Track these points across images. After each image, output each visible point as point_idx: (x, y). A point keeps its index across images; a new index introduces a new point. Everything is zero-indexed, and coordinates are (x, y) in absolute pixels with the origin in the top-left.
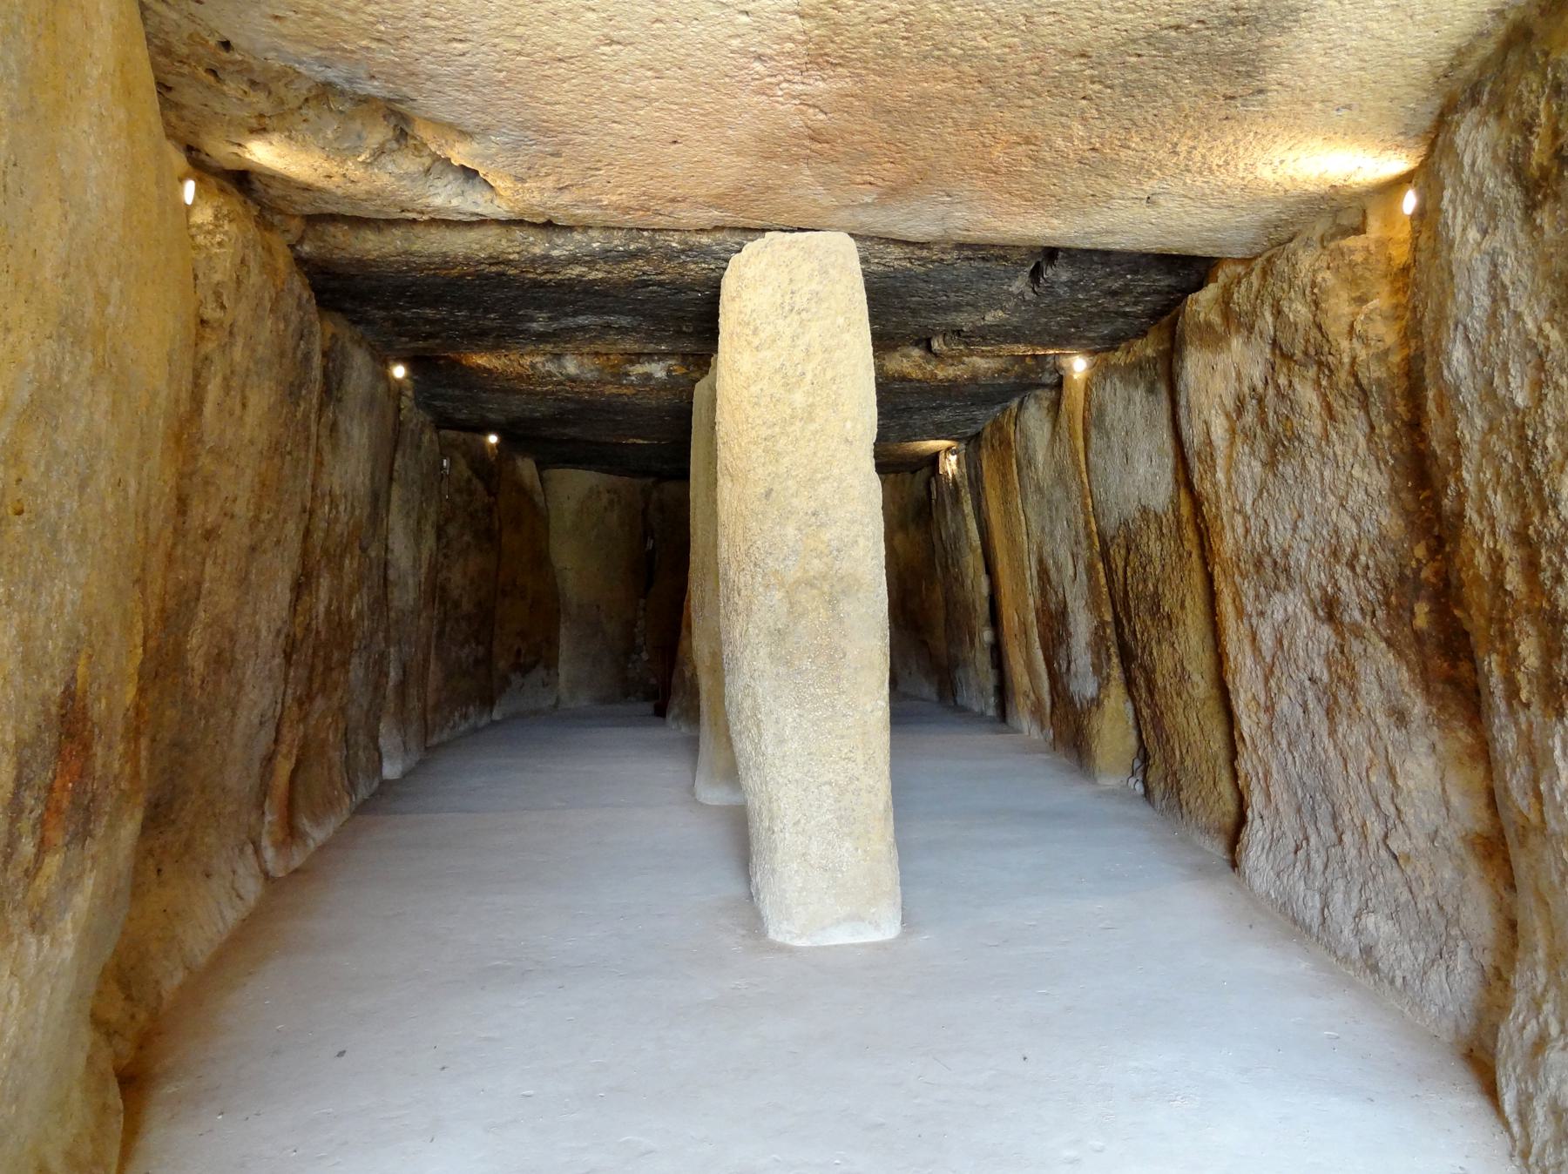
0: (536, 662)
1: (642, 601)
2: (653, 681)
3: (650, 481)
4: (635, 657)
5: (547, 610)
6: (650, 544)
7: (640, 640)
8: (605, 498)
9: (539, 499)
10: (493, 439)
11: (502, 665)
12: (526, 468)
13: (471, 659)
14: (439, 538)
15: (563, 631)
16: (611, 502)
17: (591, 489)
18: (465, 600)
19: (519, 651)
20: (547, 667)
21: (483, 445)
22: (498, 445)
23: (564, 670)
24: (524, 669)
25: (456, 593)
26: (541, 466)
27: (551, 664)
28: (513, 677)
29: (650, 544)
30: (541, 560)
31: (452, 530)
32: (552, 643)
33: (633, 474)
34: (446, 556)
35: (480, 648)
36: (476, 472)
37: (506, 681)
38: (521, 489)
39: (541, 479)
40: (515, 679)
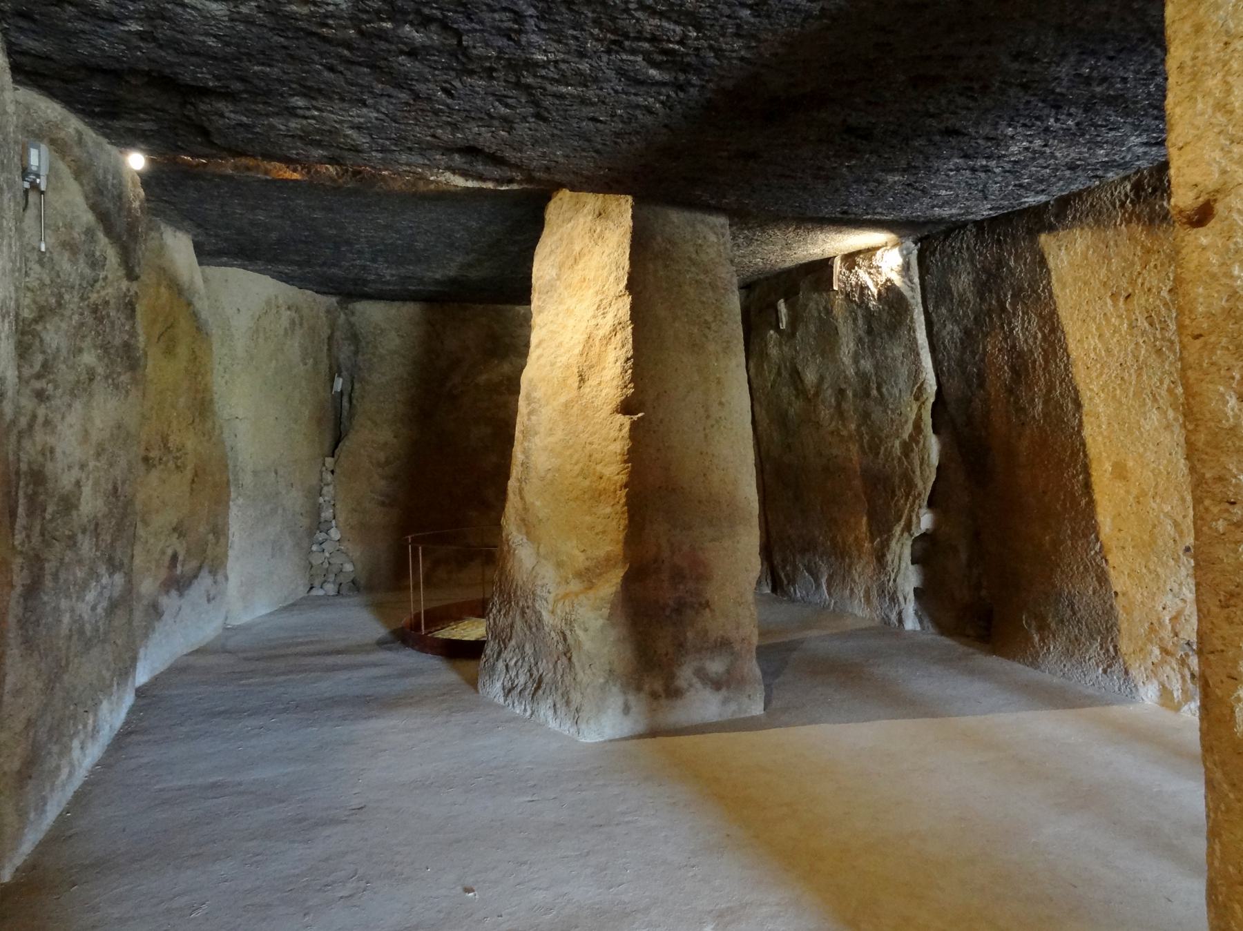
0: (200, 568)
1: (329, 460)
2: (348, 567)
3: (333, 300)
4: (321, 536)
5: (211, 482)
6: (339, 384)
7: (327, 514)
8: (286, 315)
9: (202, 305)
10: (136, 161)
11: (147, 586)
12: (178, 247)
13: (105, 604)
14: (23, 351)
15: (234, 511)
16: (293, 323)
17: (268, 303)
18: (87, 490)
19: (174, 557)
20: (213, 572)
21: (118, 171)
22: (147, 180)
23: (236, 569)
24: (178, 584)
25: (66, 482)
26: (205, 254)
27: (217, 566)
28: (164, 601)
29: (339, 384)
30: (202, 407)
31: (54, 336)
32: (219, 532)
33: (324, 285)
34: (41, 396)
35: (119, 578)
36: (103, 217)
37: (155, 611)
38: (177, 289)
39: (206, 280)
40: (169, 602)
